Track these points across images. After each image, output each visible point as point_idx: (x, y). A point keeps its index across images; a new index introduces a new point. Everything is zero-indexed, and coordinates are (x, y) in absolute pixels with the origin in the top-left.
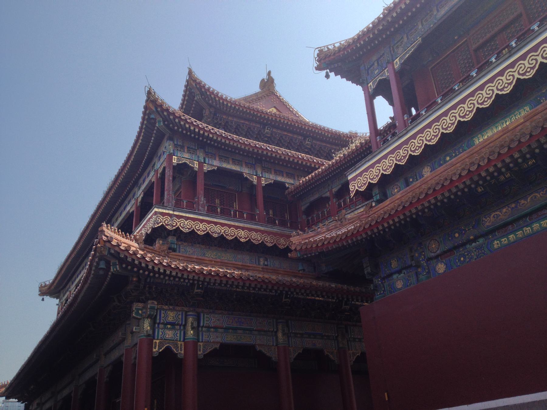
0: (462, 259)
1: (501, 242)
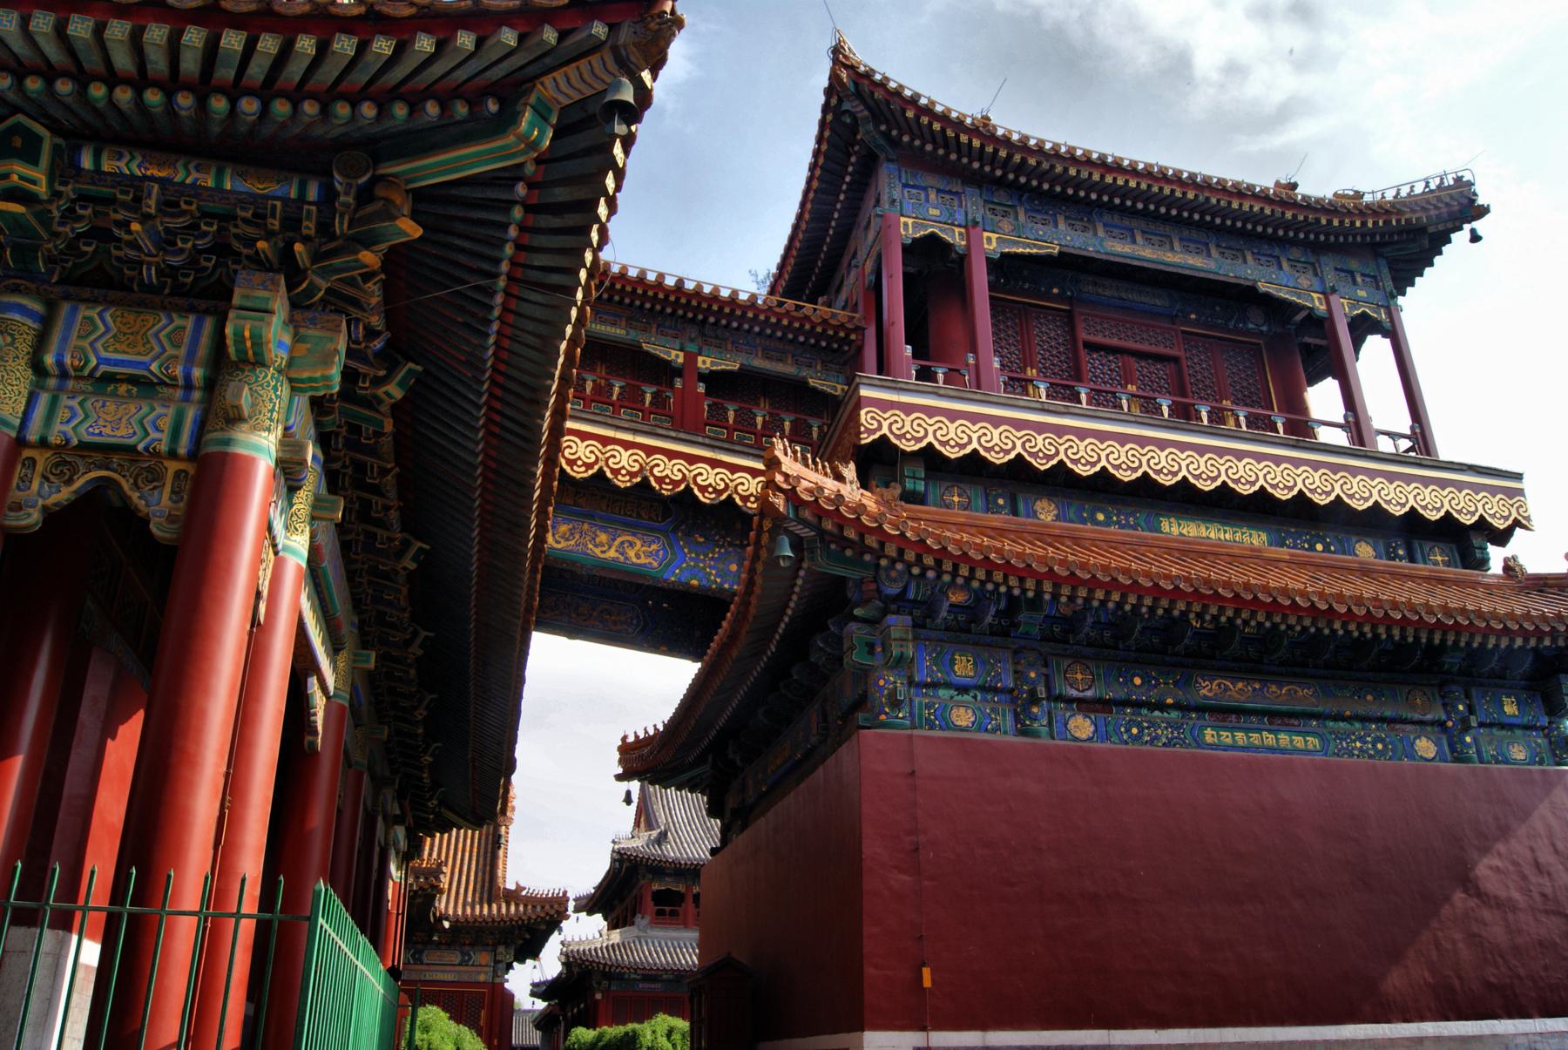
0: (1135, 731)
1: (1219, 736)
